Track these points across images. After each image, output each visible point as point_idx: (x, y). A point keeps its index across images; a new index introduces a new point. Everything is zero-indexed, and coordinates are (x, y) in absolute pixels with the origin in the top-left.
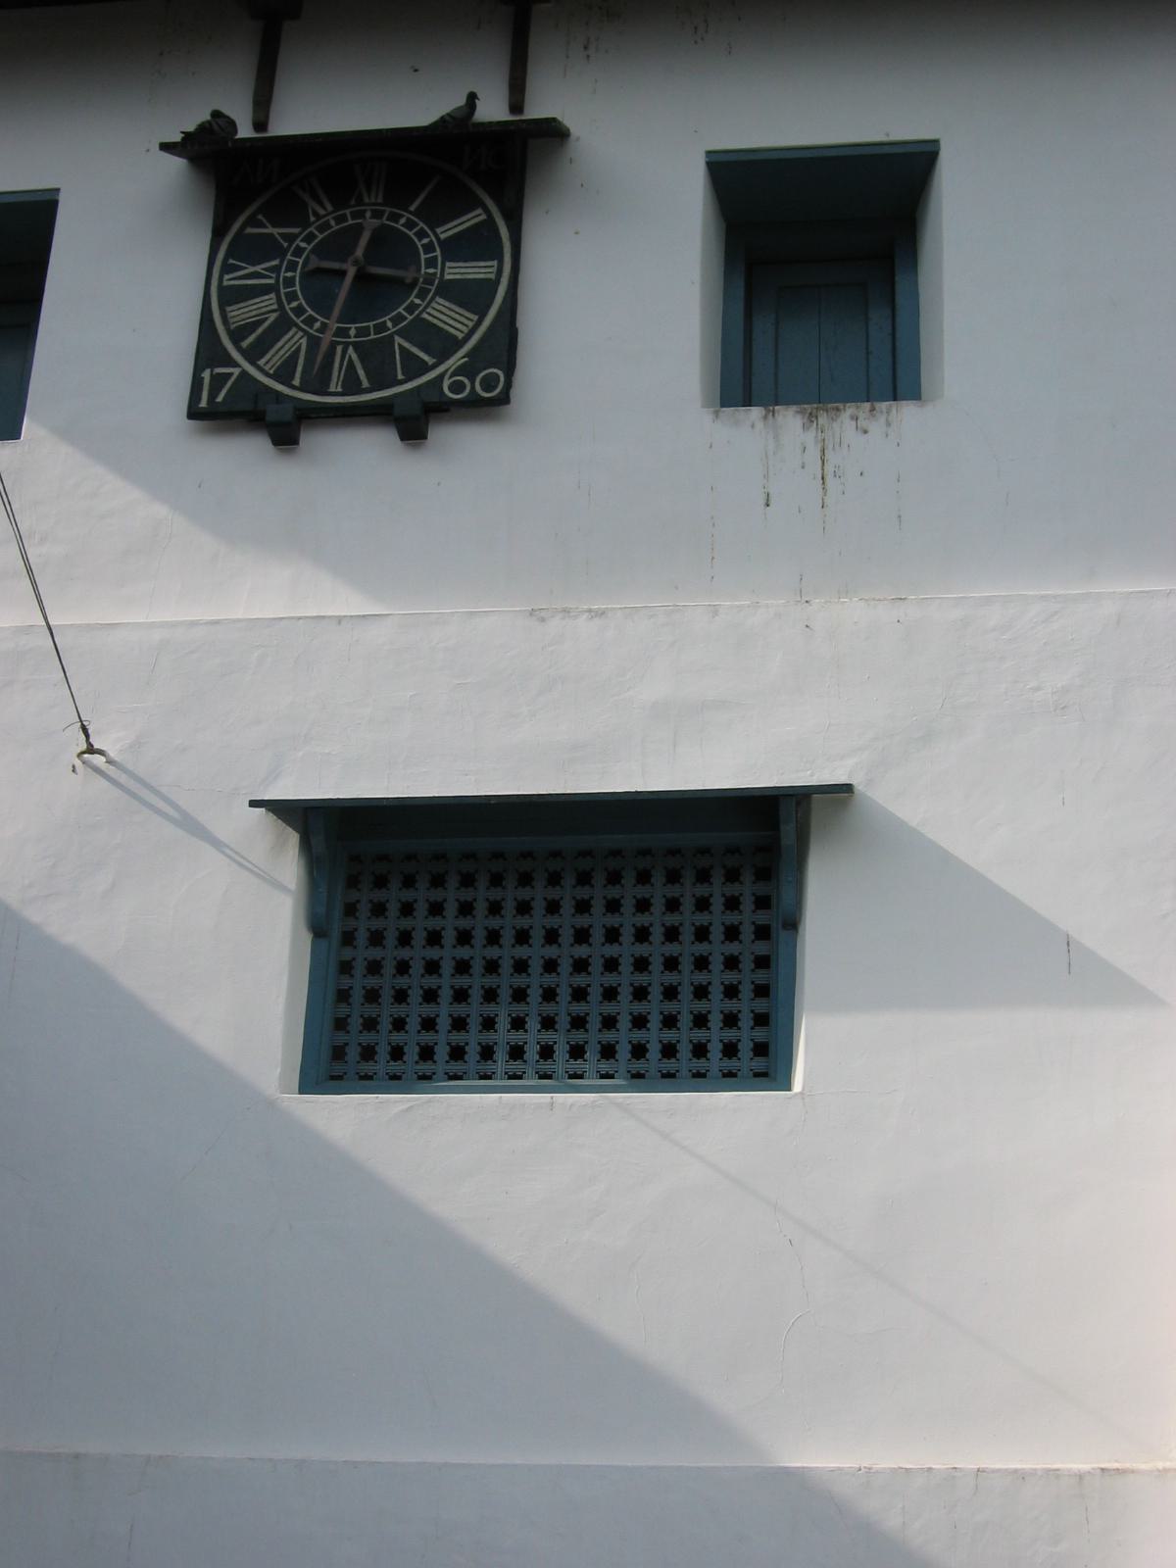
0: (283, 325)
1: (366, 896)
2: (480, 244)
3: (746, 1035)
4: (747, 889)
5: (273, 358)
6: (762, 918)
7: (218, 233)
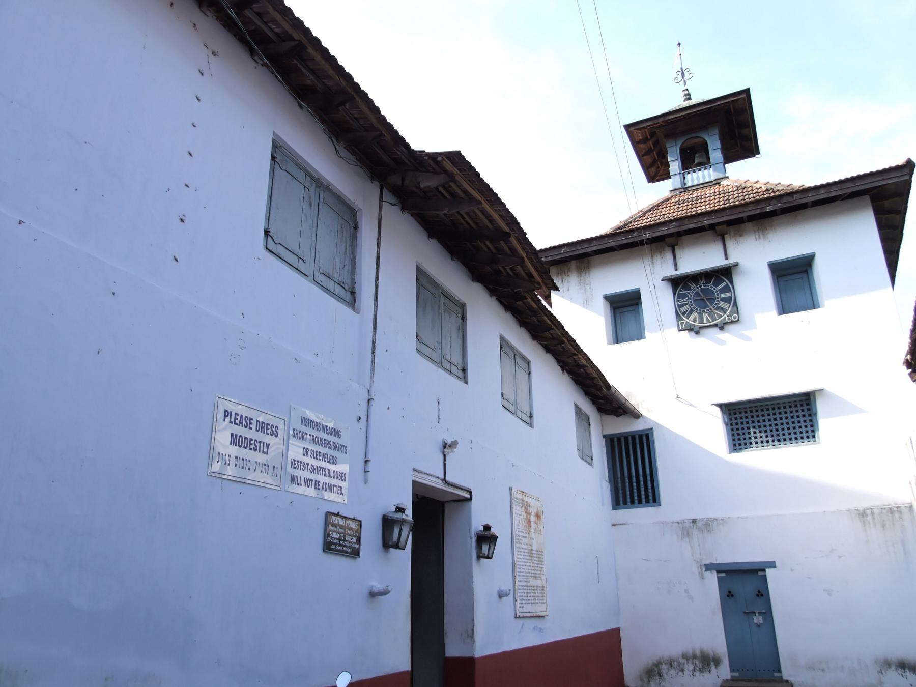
0: (691, 312)
1: (733, 416)
2: (726, 289)
3: (810, 434)
5: (692, 317)
7: (674, 294)
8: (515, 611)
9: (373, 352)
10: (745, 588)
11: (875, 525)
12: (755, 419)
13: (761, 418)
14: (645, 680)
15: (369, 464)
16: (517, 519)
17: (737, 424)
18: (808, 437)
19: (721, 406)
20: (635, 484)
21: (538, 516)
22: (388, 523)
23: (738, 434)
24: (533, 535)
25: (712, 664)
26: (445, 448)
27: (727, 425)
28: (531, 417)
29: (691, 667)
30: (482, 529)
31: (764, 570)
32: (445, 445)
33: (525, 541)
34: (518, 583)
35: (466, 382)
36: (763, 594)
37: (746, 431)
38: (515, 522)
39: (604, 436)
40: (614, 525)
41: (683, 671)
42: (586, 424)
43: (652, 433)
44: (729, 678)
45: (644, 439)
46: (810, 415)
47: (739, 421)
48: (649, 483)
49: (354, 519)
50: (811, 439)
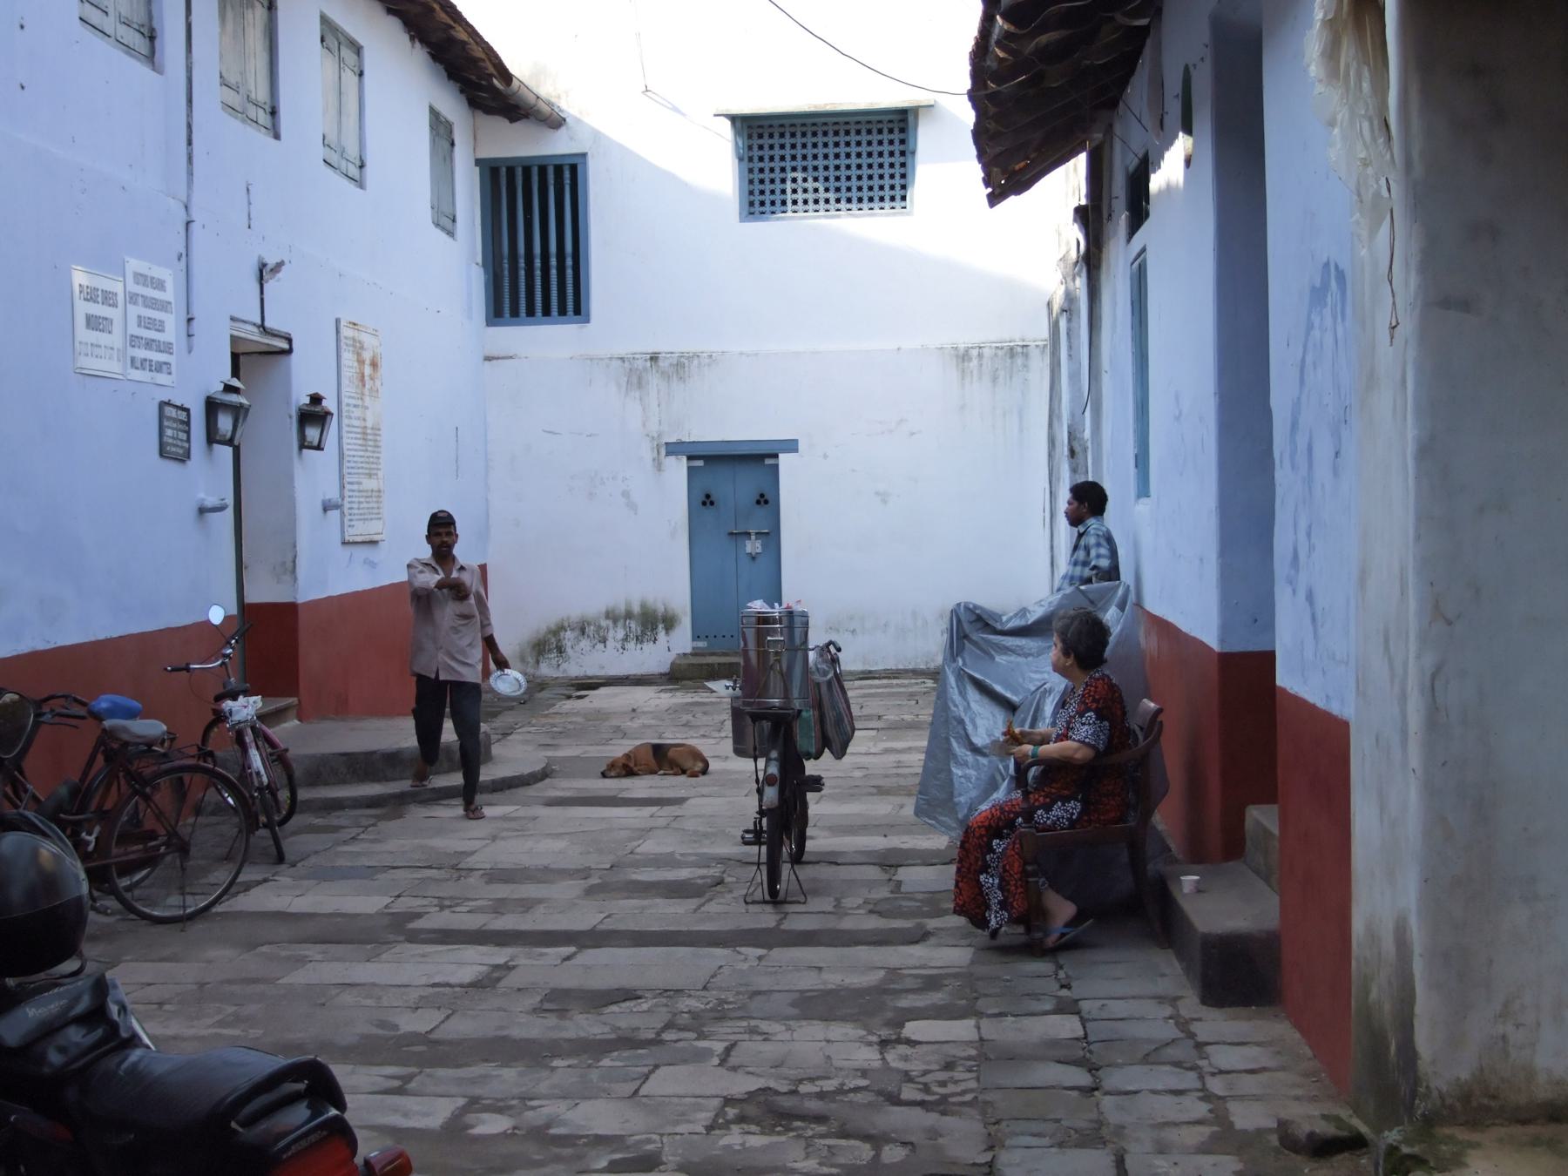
1: (756, 142)
3: (898, 193)
4: (896, 136)
6: (902, 148)
8: (343, 532)
9: (190, 143)
10: (735, 486)
11: (980, 378)
12: (799, 152)
13: (810, 151)
14: (531, 660)
15: (195, 323)
16: (346, 373)
17: (761, 159)
18: (893, 199)
19: (734, 119)
20: (538, 273)
21: (374, 365)
22: (212, 407)
23: (762, 181)
24: (367, 399)
25: (661, 626)
26: (261, 272)
27: (741, 159)
28: (362, 167)
29: (621, 634)
30: (307, 400)
31: (776, 456)
32: (262, 267)
33: (357, 412)
34: (348, 487)
35: (277, 136)
36: (767, 501)
37: (777, 175)
38: (345, 382)
39: (478, 162)
40: (488, 359)
41: (604, 641)
42: (447, 145)
43: (585, 164)
44: (689, 650)
45: (567, 174)
46: (903, 153)
47: (767, 153)
48: (569, 272)
49: (182, 408)
50: (898, 204)
